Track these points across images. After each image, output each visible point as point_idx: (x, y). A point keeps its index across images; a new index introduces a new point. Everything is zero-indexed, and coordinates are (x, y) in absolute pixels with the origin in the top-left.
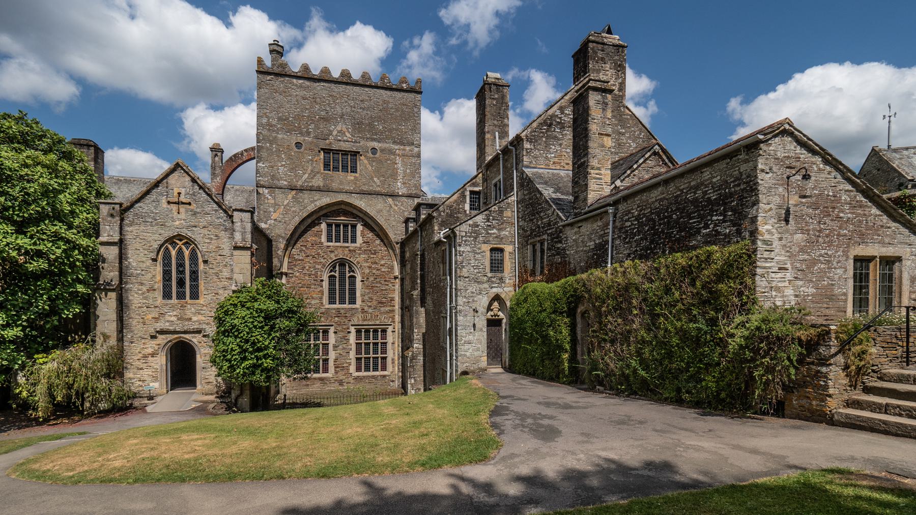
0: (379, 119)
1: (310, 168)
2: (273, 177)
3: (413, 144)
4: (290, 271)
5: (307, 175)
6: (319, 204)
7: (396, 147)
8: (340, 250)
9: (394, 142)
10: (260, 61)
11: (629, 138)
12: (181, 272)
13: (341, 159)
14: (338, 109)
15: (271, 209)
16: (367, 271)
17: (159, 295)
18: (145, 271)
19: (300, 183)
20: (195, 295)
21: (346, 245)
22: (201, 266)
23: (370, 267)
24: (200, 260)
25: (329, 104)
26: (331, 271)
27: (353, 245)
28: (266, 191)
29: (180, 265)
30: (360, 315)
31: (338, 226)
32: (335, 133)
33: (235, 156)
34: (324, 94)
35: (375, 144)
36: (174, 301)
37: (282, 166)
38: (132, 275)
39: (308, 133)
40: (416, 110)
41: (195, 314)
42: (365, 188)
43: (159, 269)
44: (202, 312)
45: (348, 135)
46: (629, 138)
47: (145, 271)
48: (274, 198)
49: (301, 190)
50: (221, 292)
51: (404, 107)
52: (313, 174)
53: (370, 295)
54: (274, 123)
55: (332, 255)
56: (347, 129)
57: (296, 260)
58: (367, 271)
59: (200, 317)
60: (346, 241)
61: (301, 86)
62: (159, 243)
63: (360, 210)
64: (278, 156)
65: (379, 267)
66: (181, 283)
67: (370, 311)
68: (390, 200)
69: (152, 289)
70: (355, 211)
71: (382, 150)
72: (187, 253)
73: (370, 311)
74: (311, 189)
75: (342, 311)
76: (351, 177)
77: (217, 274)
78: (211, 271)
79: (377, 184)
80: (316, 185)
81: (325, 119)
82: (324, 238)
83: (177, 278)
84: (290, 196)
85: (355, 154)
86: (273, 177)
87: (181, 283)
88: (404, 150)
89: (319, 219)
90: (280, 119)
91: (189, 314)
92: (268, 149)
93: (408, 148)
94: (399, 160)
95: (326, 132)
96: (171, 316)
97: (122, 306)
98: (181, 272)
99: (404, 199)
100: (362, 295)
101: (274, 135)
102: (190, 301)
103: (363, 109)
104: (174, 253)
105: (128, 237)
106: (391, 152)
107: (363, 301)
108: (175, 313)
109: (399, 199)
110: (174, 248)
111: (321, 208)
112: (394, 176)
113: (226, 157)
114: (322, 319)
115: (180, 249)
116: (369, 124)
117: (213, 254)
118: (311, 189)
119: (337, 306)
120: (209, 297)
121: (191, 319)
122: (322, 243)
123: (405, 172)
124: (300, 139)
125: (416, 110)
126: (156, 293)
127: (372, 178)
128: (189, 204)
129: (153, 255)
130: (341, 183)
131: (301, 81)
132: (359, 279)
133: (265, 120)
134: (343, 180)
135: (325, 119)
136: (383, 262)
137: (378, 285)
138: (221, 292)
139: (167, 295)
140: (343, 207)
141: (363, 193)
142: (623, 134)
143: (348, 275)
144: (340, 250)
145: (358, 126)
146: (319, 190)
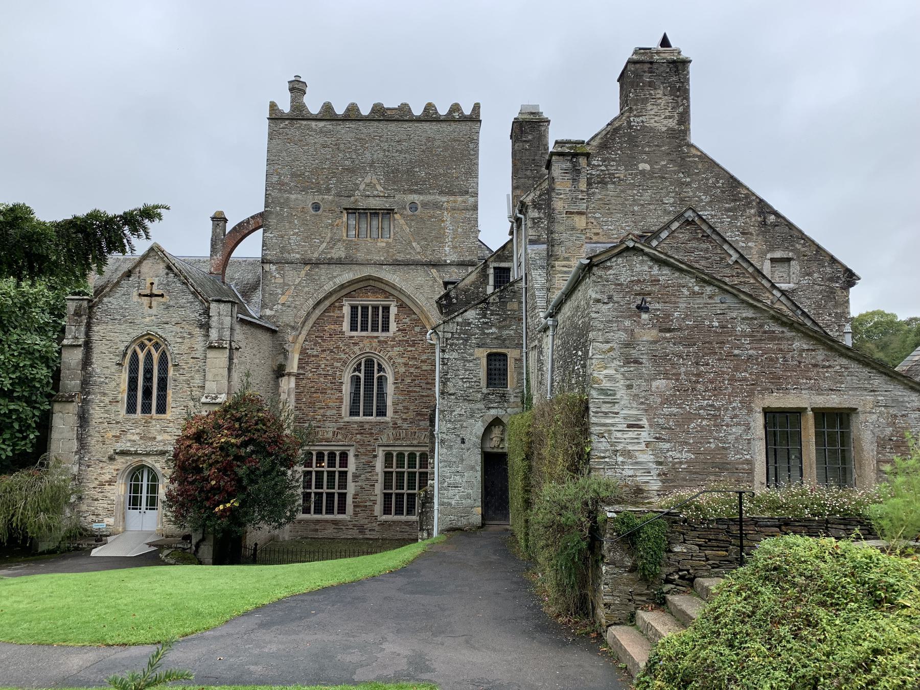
1: (329, 235)
2: (283, 250)
3: (467, 193)
4: (301, 372)
5: (325, 245)
6: (339, 281)
7: (444, 199)
8: (366, 342)
9: (441, 193)
10: (273, 106)
11: (698, 189)
12: (148, 379)
14: (368, 155)
15: (279, 291)
16: (402, 370)
17: (122, 408)
18: (111, 379)
19: (316, 255)
20: (162, 409)
21: (375, 334)
22: (171, 372)
23: (406, 364)
25: (355, 150)
26: (354, 371)
27: (384, 334)
28: (273, 267)
29: (148, 371)
30: (390, 432)
31: (365, 308)
32: (362, 187)
33: (239, 225)
34: (349, 137)
35: (416, 198)
36: (139, 415)
38: (95, 384)
39: (328, 190)
40: (472, 146)
41: (159, 432)
42: (400, 257)
43: (125, 376)
44: (169, 430)
45: (379, 188)
46: (698, 189)
47: (111, 379)
48: (283, 277)
49: (317, 264)
51: (455, 144)
53: (405, 404)
55: (356, 349)
56: (379, 180)
57: (309, 356)
58: (402, 370)
60: (375, 329)
62: (126, 344)
63: (394, 287)
64: (290, 222)
65: (418, 364)
66: (147, 393)
67: (405, 426)
68: (434, 271)
69: (115, 401)
70: (387, 289)
71: (425, 205)
72: (156, 356)
73: (405, 426)
74: (330, 262)
75: (367, 426)
77: (188, 382)
78: (182, 378)
79: (416, 251)
80: (336, 256)
81: (352, 171)
82: (346, 326)
83: (144, 386)
84: (303, 272)
86: (283, 250)
87: (147, 393)
88: (455, 202)
89: (339, 300)
90: (293, 175)
92: (278, 214)
93: (460, 199)
94: (447, 216)
95: (350, 186)
97: (83, 419)
98: (148, 379)
100: (394, 404)
101: (286, 196)
104: (141, 356)
105: (95, 337)
106: (437, 206)
107: (395, 412)
108: (138, 431)
110: (142, 350)
111: (342, 287)
112: (440, 238)
113: (229, 227)
114: (340, 437)
115: (149, 352)
118: (330, 262)
119: (361, 418)
120: (178, 411)
121: (155, 438)
122: (343, 333)
123: (455, 231)
124: (318, 198)
125: (472, 146)
126: (119, 405)
127: (410, 242)
131: (321, 124)
132: (390, 379)
133: (275, 179)
135: (352, 171)
136: (424, 357)
137: (418, 389)
139: (131, 409)
140: (372, 283)
141: (397, 264)
142: (688, 184)
143: (376, 375)
144: (366, 341)
146: (339, 262)
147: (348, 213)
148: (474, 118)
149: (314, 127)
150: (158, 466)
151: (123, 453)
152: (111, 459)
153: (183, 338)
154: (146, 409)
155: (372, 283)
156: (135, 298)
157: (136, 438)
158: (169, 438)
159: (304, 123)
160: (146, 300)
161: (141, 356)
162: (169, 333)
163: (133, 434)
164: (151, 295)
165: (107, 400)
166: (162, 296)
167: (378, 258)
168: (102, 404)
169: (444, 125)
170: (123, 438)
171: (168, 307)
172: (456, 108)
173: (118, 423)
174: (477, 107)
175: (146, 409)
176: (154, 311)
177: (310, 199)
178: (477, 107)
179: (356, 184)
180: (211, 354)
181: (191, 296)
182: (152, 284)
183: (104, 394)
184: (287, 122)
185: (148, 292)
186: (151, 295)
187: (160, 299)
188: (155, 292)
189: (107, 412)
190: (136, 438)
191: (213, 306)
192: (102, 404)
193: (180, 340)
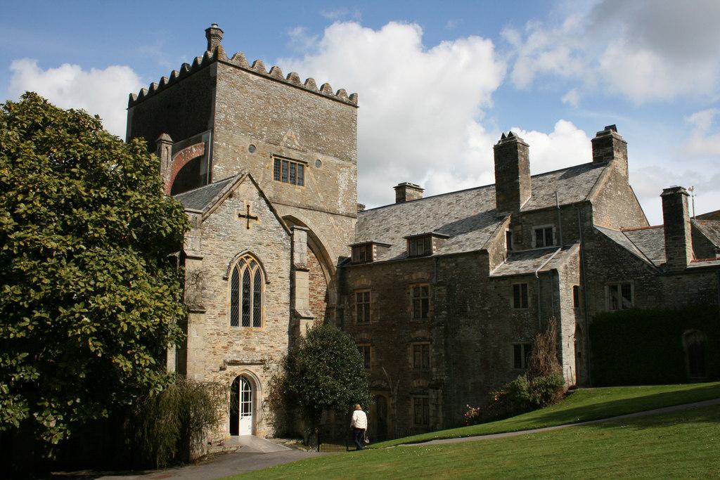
0: (323, 130)
9: (336, 156)
12: (246, 295)
13: (288, 170)
14: (289, 114)
17: (228, 319)
20: (257, 323)
22: (264, 288)
29: (247, 287)
32: (285, 139)
35: (320, 156)
36: (240, 328)
40: (353, 125)
42: (311, 203)
43: (229, 289)
50: (280, 318)
54: (231, 119)
56: (296, 136)
59: (263, 348)
61: (256, 83)
66: (246, 309)
69: (222, 314)
72: (253, 273)
79: (319, 200)
81: (277, 123)
85: (303, 164)
87: (246, 309)
90: (236, 116)
91: (253, 345)
96: (237, 345)
99: (344, 219)
102: (254, 329)
103: (310, 117)
104: (242, 272)
108: (241, 342)
116: (315, 133)
117: (274, 276)
120: (271, 324)
121: (254, 349)
128: (256, 218)
129: (223, 274)
130: (290, 196)
131: (257, 78)
134: (289, 192)
135: (277, 123)
136: (319, 289)
138: (280, 318)
139: (234, 322)
145: (309, 135)
147: (275, 159)
148: (352, 102)
149: (251, 78)
150: (258, 374)
152: (222, 369)
153: (272, 258)
154: (246, 323)
157: (240, 348)
158: (265, 349)
159: (245, 73)
160: (244, 221)
161: (242, 272)
163: (237, 345)
165: (217, 312)
167: (296, 202)
168: (213, 317)
170: (230, 350)
171: (261, 229)
173: (225, 334)
176: (249, 232)
177: (246, 142)
179: (280, 136)
180: (298, 275)
182: (248, 206)
183: (214, 307)
184: (232, 68)
185: (245, 213)
186: (249, 217)
187: (254, 221)
188: (252, 214)
189: (217, 323)
190: (240, 348)
192: (213, 317)
193: (270, 260)
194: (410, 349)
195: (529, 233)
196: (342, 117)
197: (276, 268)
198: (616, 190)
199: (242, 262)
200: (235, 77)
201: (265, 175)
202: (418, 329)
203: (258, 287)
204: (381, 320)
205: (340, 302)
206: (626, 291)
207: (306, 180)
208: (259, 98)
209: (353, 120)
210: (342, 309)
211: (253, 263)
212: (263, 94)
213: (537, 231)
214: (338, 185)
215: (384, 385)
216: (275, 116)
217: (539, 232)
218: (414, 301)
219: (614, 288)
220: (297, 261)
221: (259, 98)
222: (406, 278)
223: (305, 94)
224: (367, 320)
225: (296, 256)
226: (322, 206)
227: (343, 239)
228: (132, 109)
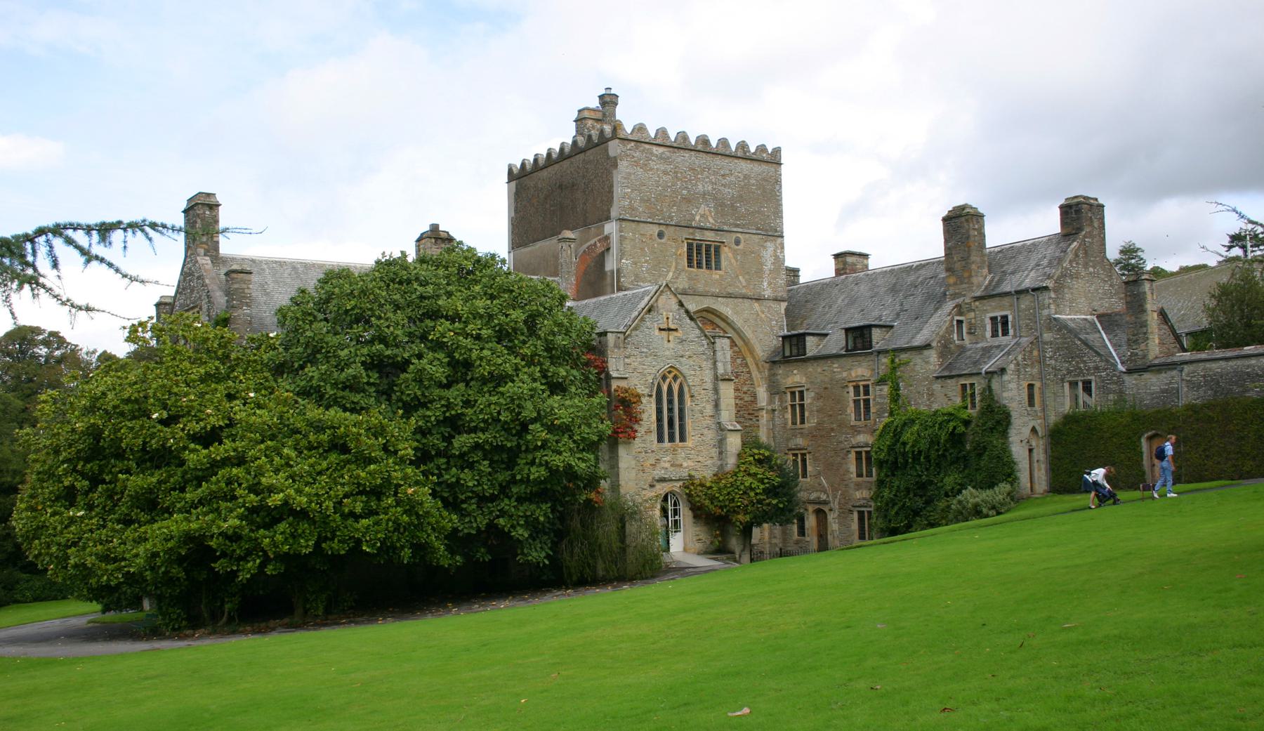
12: (670, 410)
17: (654, 437)
20: (682, 439)
22: (688, 402)
24: (687, 396)
29: (670, 402)
32: (697, 218)
36: (667, 444)
37: (646, 261)
42: (730, 290)
52: (678, 272)
59: (690, 463)
61: (661, 158)
63: (724, 319)
69: (649, 432)
70: (717, 321)
72: (676, 388)
76: (716, 275)
79: (742, 285)
80: (681, 287)
81: (687, 200)
91: (680, 461)
98: (670, 410)
103: (724, 186)
104: (665, 388)
108: (668, 458)
109: (765, 303)
112: (760, 272)
131: (661, 150)
134: (706, 278)
136: (745, 389)
138: (706, 431)
139: (660, 440)
148: (772, 159)
151: (662, 480)
152: (652, 486)
154: (672, 439)
155: (704, 314)
156: (657, 332)
157: (667, 465)
159: (647, 146)
161: (665, 388)
162: (685, 367)
164: (670, 330)
166: (676, 330)
169: (756, 164)
171: (682, 341)
172: (762, 148)
174: (777, 151)
175: (672, 439)
176: (671, 345)
178: (777, 151)
181: (697, 331)
185: (664, 326)
186: (670, 330)
187: (675, 333)
188: (672, 327)
190: (667, 465)
191: (717, 340)
194: (852, 456)
195: (982, 321)
196: (764, 179)
197: (698, 376)
198: (1086, 266)
199: (664, 378)
200: (637, 154)
201: (677, 264)
202: (859, 433)
203: (681, 401)
204: (818, 423)
205: (771, 401)
206: (1087, 388)
207: (724, 263)
208: (665, 173)
209: (777, 181)
210: (774, 410)
211: (675, 378)
212: (669, 168)
213: (992, 319)
214: (762, 264)
215: (824, 497)
216: (685, 192)
217: (993, 319)
218: (855, 401)
219: (1073, 385)
220: (721, 371)
221: (665, 173)
222: (845, 374)
223: (718, 161)
224: (802, 422)
225: (720, 365)
226: (744, 291)
227: (771, 327)
228: (514, 183)
